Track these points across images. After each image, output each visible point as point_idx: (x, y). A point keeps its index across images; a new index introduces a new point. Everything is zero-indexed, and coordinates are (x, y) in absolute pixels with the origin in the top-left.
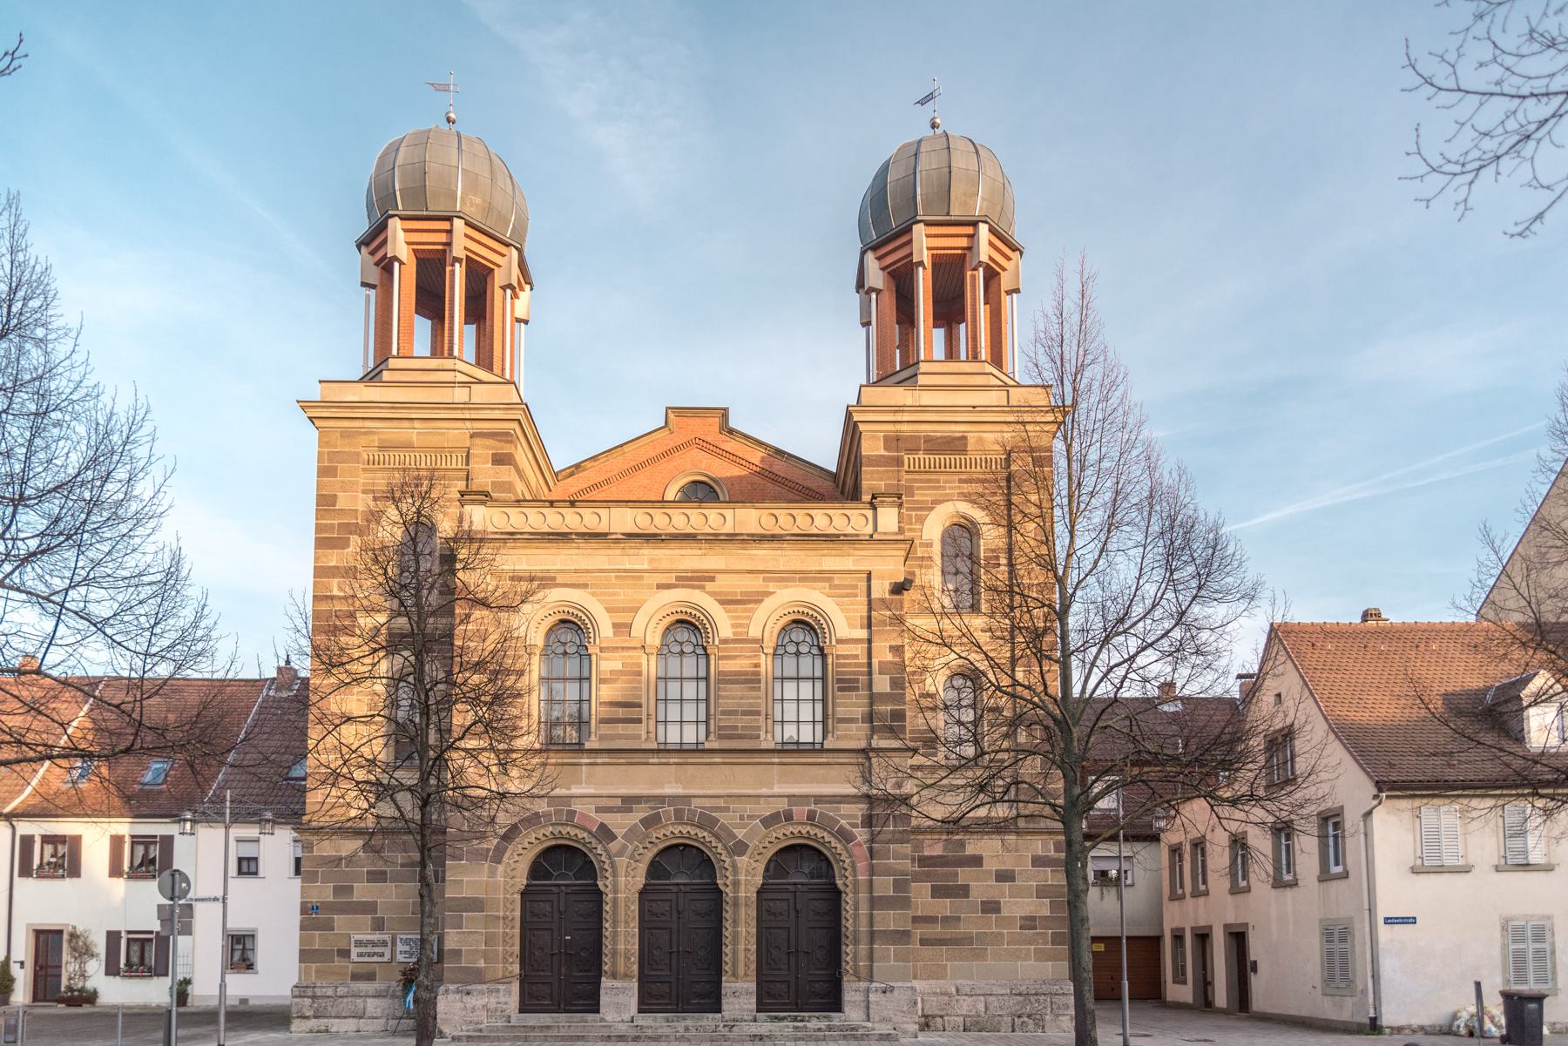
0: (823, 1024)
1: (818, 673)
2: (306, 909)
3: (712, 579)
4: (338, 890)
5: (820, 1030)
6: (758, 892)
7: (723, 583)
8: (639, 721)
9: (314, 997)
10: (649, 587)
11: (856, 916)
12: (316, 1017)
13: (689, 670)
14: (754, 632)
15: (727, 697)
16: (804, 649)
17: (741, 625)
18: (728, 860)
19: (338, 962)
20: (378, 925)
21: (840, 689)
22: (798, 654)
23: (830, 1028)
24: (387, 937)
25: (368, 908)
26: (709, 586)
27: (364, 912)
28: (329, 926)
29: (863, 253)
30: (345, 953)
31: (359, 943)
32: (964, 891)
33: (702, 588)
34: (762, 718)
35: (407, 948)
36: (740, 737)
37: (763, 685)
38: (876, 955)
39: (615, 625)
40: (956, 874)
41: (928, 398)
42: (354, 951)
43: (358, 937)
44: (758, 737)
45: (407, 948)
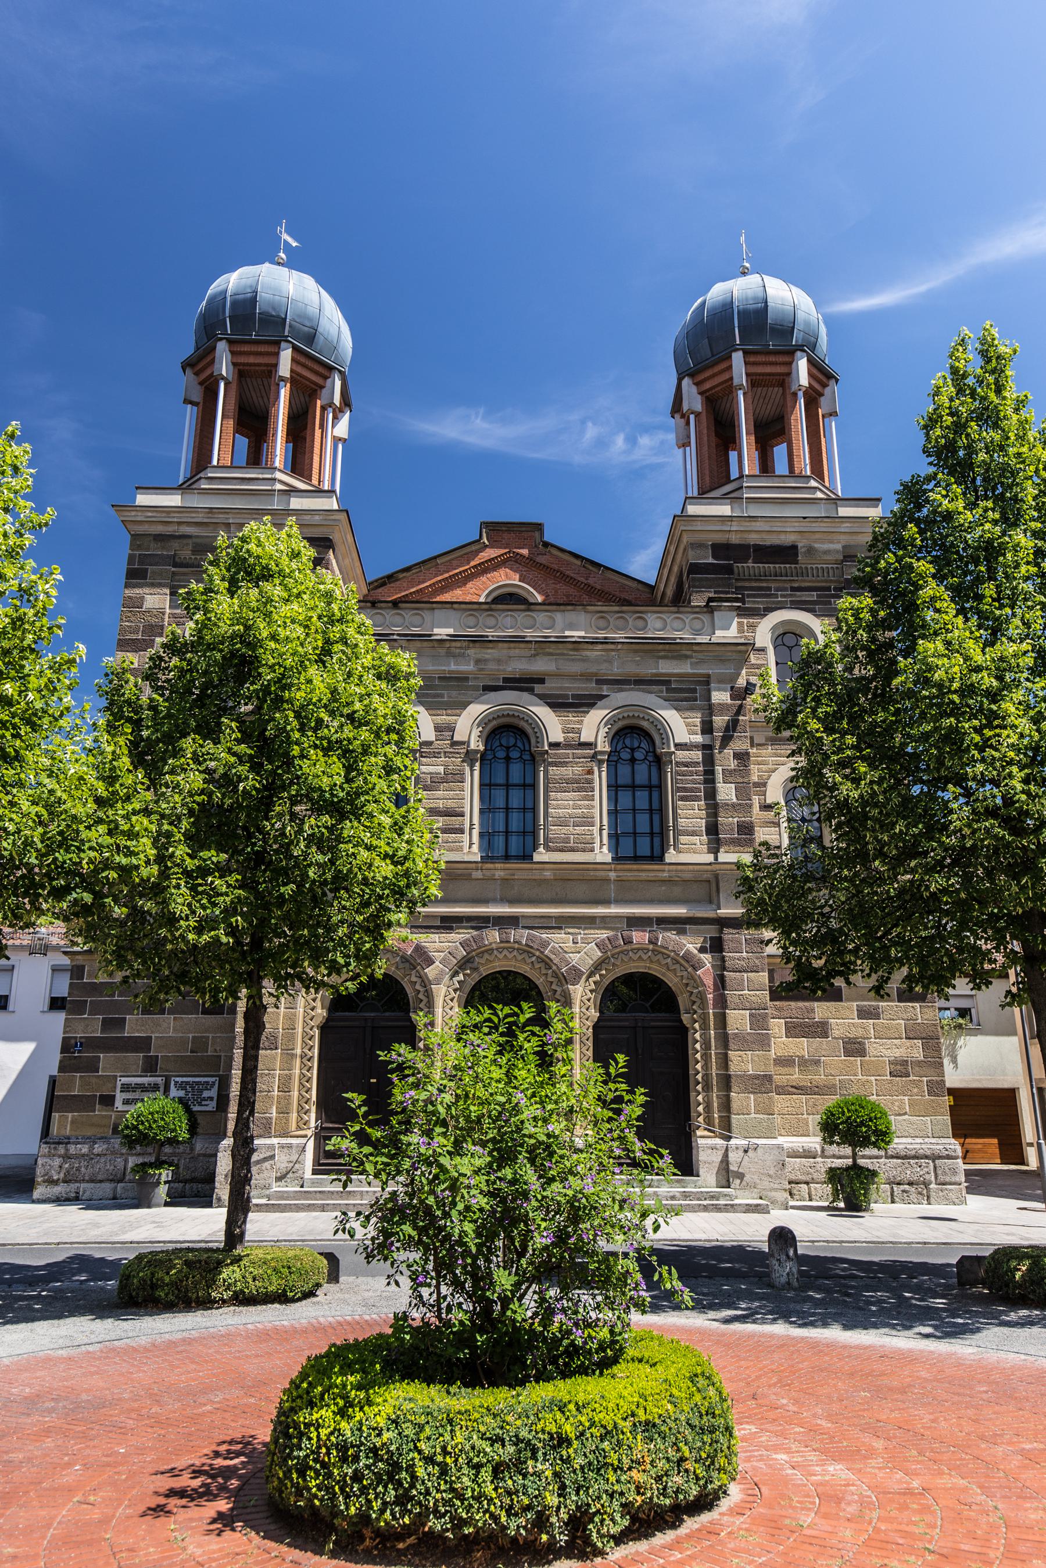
0: (677, 1190)
1: (655, 781)
2: (67, 1046)
3: (541, 681)
4: (107, 1024)
5: (673, 1198)
6: (596, 1027)
7: (551, 686)
8: (461, 831)
9: (67, 1157)
10: (475, 688)
11: (706, 1057)
12: (65, 1181)
13: (516, 777)
14: (586, 736)
15: (558, 807)
16: (639, 755)
17: (573, 731)
18: (559, 989)
19: (99, 1111)
20: (150, 1066)
21: (682, 799)
22: (633, 760)
23: (686, 1196)
24: (159, 1080)
25: (142, 1044)
26: (538, 688)
27: (136, 1050)
28: (92, 1066)
29: (680, 381)
30: (108, 1101)
31: (126, 1088)
32: (821, 1030)
33: (531, 691)
34: (596, 830)
35: (182, 1093)
36: (572, 850)
37: (597, 793)
38: (735, 1105)
39: (438, 729)
40: (813, 1010)
41: (754, 511)
42: (120, 1098)
43: (124, 1080)
44: (592, 850)
45: (182, 1093)
